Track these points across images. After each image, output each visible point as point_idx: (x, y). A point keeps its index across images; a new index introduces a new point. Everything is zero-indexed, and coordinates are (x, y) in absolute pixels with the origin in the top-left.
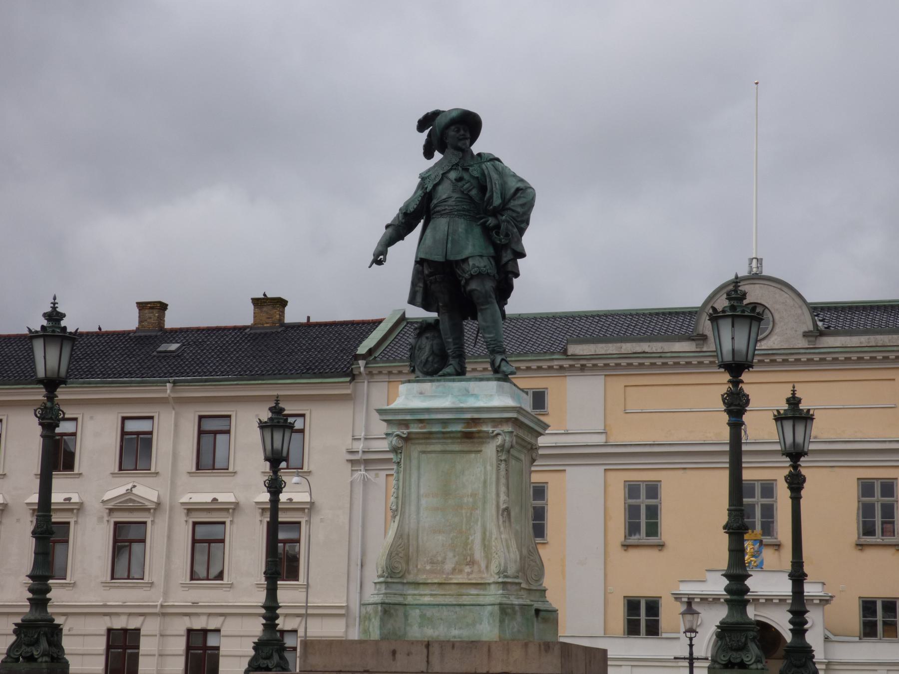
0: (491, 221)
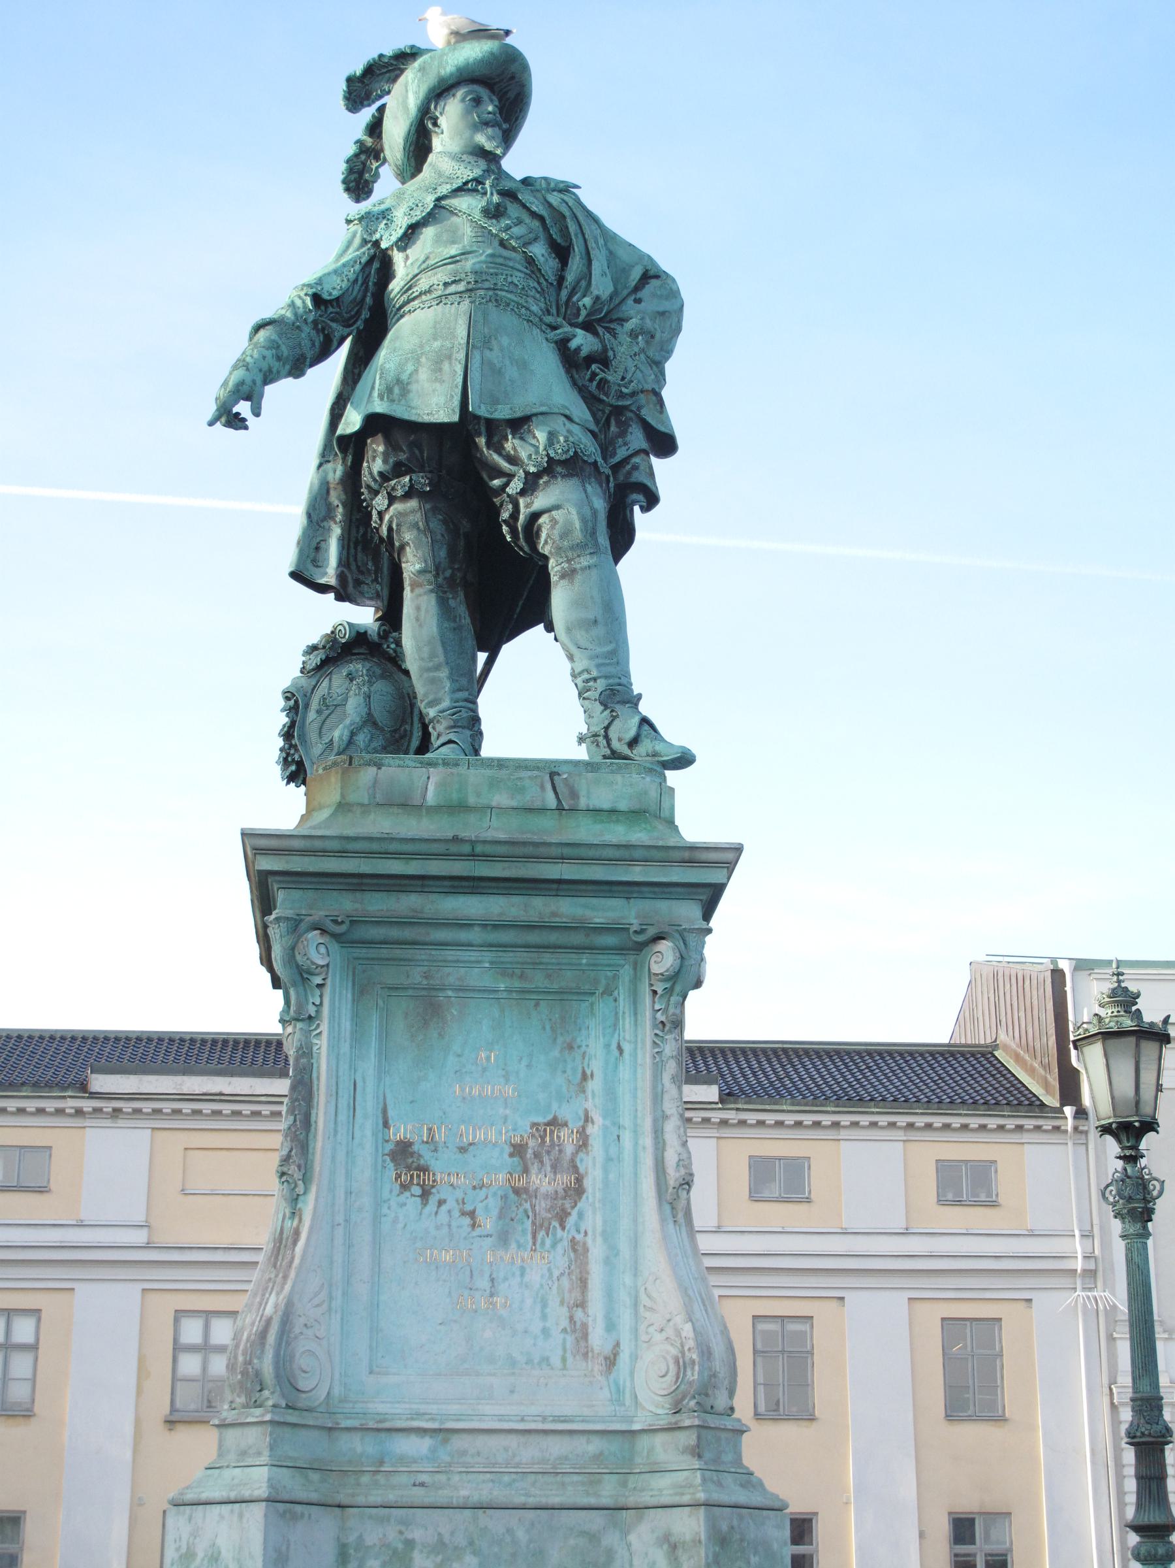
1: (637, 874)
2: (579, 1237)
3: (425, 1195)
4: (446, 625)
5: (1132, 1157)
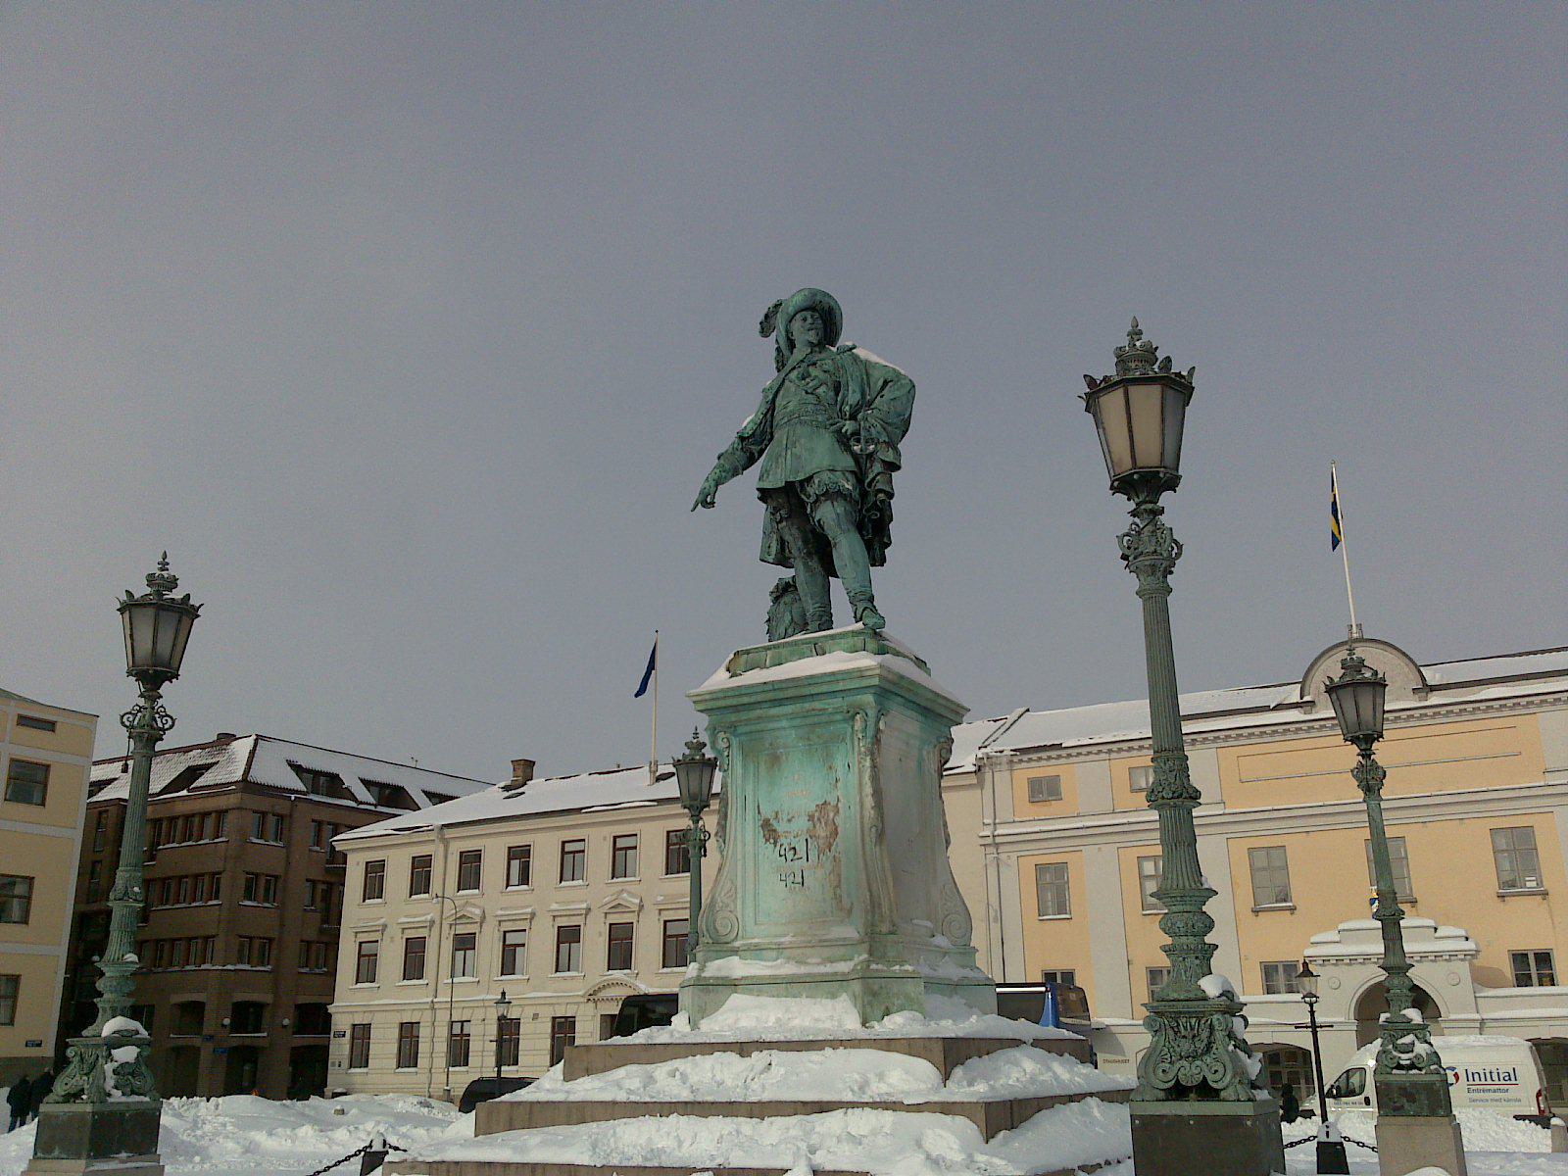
0: (849, 426)
1: (841, 686)
3: (775, 843)
4: (807, 574)
5: (1366, 754)
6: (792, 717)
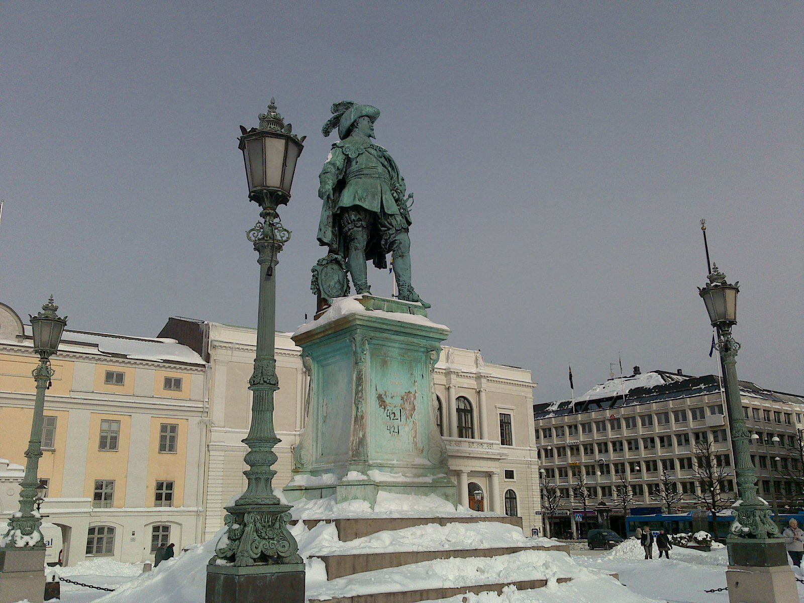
1: (431, 335)
2: (415, 421)
3: (385, 408)
6: (401, 342)
